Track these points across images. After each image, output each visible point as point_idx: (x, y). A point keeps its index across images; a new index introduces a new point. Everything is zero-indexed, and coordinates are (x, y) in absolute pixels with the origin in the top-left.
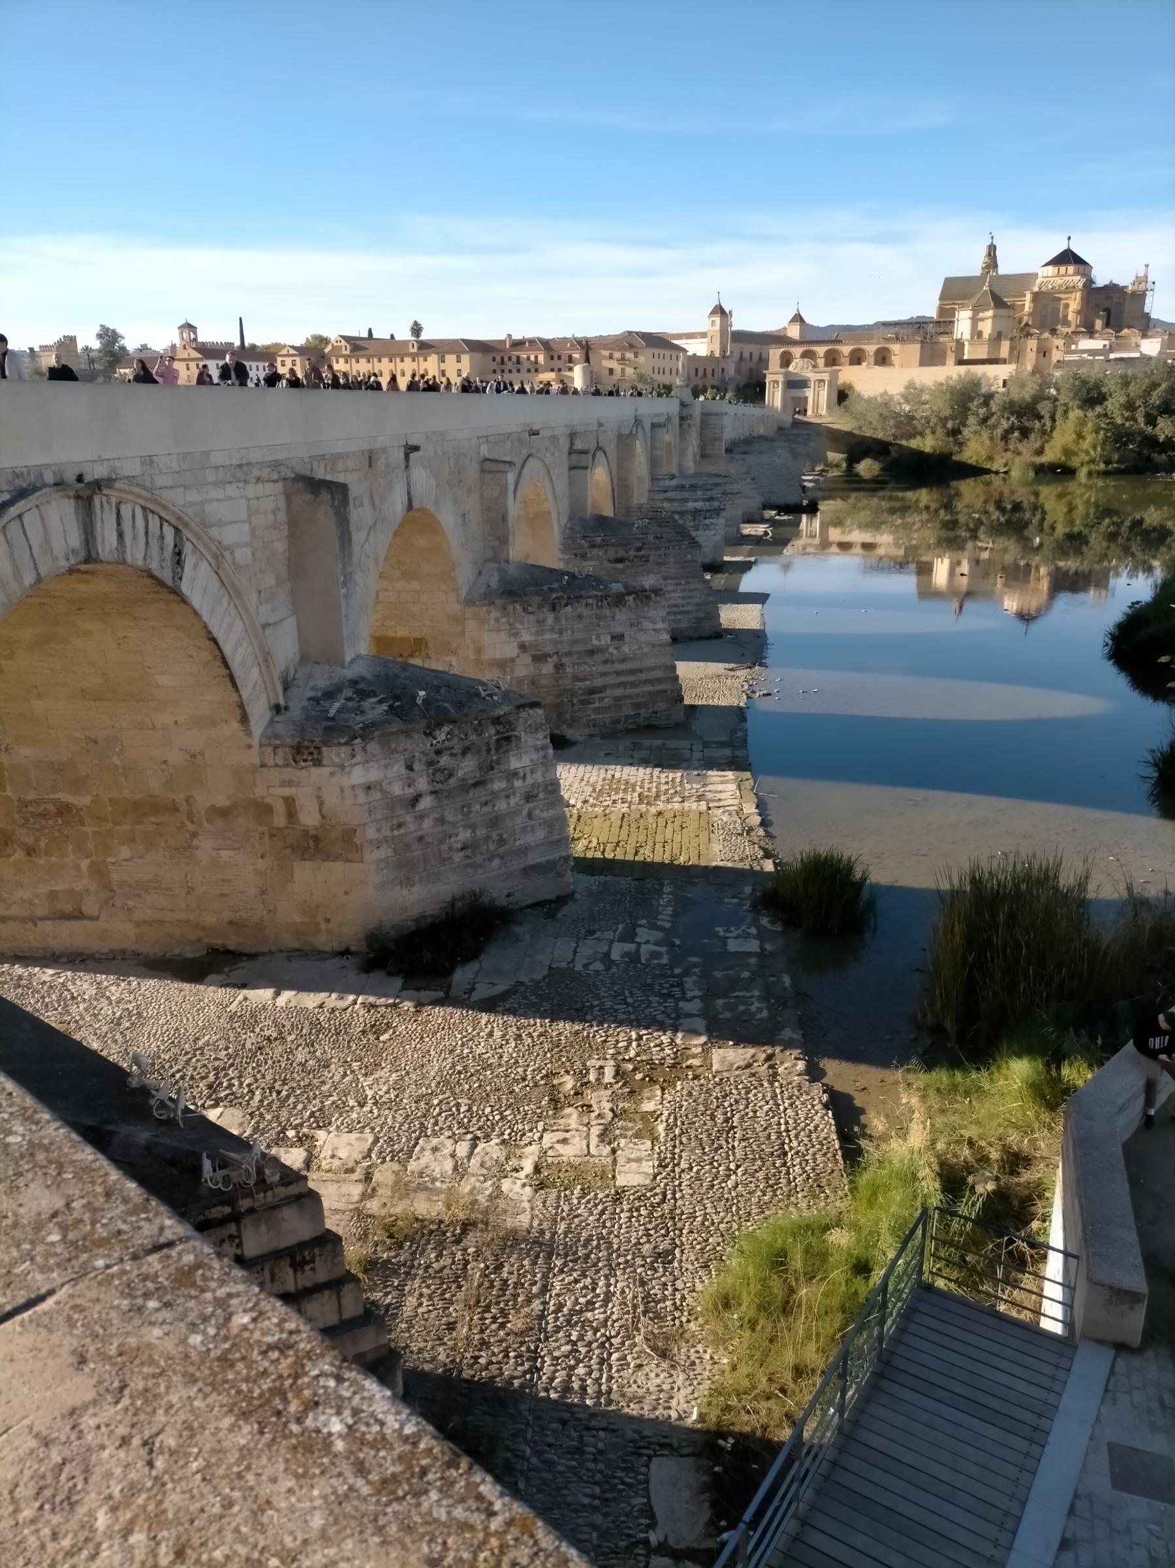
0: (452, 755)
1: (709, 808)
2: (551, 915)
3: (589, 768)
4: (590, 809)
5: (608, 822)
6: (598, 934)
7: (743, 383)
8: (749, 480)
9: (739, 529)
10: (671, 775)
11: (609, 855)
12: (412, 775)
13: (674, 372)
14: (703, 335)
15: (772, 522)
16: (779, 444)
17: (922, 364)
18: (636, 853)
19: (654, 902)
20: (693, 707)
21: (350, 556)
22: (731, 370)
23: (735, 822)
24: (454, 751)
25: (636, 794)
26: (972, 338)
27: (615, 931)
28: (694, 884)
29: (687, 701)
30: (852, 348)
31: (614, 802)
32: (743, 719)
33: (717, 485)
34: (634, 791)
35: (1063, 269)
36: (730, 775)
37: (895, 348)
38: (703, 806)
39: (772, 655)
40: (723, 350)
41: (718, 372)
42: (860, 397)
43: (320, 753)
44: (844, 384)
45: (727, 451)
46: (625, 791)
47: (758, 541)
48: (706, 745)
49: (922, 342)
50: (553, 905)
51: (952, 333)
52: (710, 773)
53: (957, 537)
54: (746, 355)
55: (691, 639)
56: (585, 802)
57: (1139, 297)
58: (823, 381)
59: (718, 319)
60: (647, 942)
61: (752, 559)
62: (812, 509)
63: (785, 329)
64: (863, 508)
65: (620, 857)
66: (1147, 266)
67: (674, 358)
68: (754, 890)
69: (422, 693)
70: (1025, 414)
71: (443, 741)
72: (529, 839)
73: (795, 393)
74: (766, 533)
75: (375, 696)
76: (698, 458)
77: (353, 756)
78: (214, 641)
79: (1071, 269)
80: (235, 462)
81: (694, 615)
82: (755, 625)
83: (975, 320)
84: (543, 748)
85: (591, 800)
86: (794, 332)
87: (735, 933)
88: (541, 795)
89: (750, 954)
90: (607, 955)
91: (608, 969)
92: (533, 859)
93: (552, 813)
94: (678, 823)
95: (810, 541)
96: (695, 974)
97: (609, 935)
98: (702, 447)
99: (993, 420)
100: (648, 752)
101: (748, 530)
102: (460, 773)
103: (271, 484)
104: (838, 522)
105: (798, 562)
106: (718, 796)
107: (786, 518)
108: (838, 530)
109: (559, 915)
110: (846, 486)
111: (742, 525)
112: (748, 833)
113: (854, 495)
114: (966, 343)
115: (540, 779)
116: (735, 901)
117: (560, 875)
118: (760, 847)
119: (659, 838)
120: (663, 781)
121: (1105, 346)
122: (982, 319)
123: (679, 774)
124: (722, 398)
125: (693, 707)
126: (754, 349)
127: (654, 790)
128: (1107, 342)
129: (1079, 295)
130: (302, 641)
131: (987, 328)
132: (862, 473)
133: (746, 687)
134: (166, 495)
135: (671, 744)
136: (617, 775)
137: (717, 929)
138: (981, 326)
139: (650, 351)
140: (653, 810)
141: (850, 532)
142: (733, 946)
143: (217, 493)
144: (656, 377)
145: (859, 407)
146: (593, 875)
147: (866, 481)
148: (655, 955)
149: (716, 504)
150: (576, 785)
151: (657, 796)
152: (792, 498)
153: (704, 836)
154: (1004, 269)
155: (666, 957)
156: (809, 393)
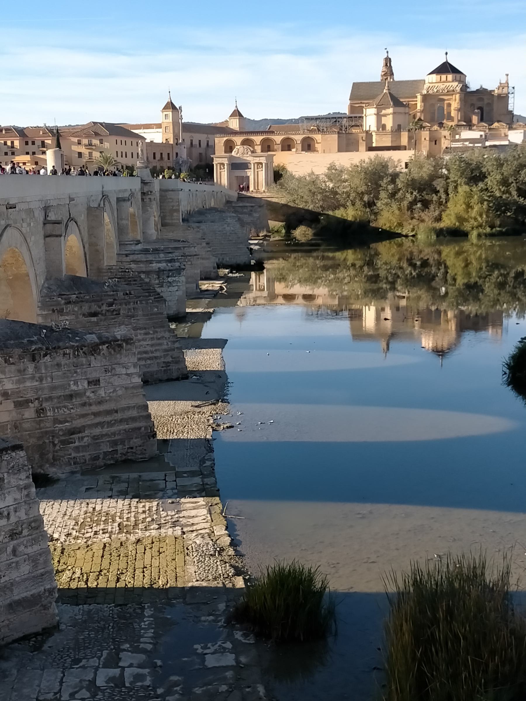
1: (184, 533)
2: (37, 648)
3: (71, 502)
4: (73, 541)
5: (90, 553)
6: (84, 662)
7: (194, 165)
8: (204, 244)
9: (198, 286)
10: (148, 505)
11: (92, 584)
13: (135, 155)
14: (159, 126)
15: (227, 279)
16: (229, 214)
17: (340, 150)
18: (118, 580)
19: (136, 626)
20: (165, 442)
22: (184, 154)
23: (208, 544)
25: (116, 524)
26: (378, 130)
27: (99, 658)
28: (172, 606)
29: (160, 436)
30: (283, 137)
31: (96, 533)
32: (211, 450)
33: (176, 248)
34: (114, 521)
35: (444, 77)
36: (201, 501)
37: (318, 137)
38: (178, 531)
39: (233, 392)
40: (176, 138)
41: (173, 157)
42: (292, 177)
44: (278, 166)
45: (183, 220)
46: (106, 522)
47: (215, 294)
48: (178, 475)
49: (339, 133)
50: (39, 638)
51: (362, 126)
52: (183, 500)
53: (379, 289)
54: (196, 142)
55: (161, 381)
56: (68, 535)
57: (504, 98)
58: (261, 164)
59: (170, 114)
60: (131, 666)
61: (211, 310)
62: (259, 268)
63: (227, 121)
64: (302, 266)
65: (102, 584)
66: (507, 75)
67: (134, 144)
68: (227, 606)
70: (424, 189)
72: (14, 575)
73: (239, 173)
74: (221, 288)
76: (159, 226)
79: (450, 77)
81: (163, 360)
82: (216, 366)
83: (379, 116)
84: (26, 487)
85: (74, 533)
86: (235, 125)
87: (212, 650)
88: (25, 532)
89: (226, 668)
90: (93, 682)
91: (94, 696)
92: (18, 594)
93: (36, 548)
94: (155, 549)
95: (259, 294)
96: (176, 692)
97: (94, 662)
98: (163, 218)
99: (399, 195)
100: (126, 485)
101: (206, 285)
104: (282, 278)
105: (251, 312)
106: (191, 521)
107: (237, 275)
108: (283, 284)
109: (45, 647)
110: (286, 248)
111: (200, 282)
112: (219, 554)
113: (293, 255)
114: (374, 134)
115: (24, 517)
116: (211, 618)
117: (45, 607)
118: (231, 565)
119: (139, 564)
120: (140, 510)
121: (481, 136)
122: (385, 115)
123: (155, 503)
124: (177, 177)
125: (165, 441)
126: (203, 137)
127: (133, 519)
128: (482, 133)
129: (458, 96)
131: (389, 122)
132: (298, 237)
133: (211, 421)
135: (146, 475)
136: (98, 508)
137: (196, 646)
138: (384, 120)
139: (113, 138)
140: (132, 538)
141: (292, 286)
142: (211, 662)
144: (119, 159)
145: (292, 185)
146: (77, 605)
147: (302, 244)
148: (139, 677)
149: (177, 264)
150: (59, 520)
151: (136, 525)
152: (242, 259)
153: (179, 558)
154: (398, 77)
155: (148, 678)
156: (250, 173)
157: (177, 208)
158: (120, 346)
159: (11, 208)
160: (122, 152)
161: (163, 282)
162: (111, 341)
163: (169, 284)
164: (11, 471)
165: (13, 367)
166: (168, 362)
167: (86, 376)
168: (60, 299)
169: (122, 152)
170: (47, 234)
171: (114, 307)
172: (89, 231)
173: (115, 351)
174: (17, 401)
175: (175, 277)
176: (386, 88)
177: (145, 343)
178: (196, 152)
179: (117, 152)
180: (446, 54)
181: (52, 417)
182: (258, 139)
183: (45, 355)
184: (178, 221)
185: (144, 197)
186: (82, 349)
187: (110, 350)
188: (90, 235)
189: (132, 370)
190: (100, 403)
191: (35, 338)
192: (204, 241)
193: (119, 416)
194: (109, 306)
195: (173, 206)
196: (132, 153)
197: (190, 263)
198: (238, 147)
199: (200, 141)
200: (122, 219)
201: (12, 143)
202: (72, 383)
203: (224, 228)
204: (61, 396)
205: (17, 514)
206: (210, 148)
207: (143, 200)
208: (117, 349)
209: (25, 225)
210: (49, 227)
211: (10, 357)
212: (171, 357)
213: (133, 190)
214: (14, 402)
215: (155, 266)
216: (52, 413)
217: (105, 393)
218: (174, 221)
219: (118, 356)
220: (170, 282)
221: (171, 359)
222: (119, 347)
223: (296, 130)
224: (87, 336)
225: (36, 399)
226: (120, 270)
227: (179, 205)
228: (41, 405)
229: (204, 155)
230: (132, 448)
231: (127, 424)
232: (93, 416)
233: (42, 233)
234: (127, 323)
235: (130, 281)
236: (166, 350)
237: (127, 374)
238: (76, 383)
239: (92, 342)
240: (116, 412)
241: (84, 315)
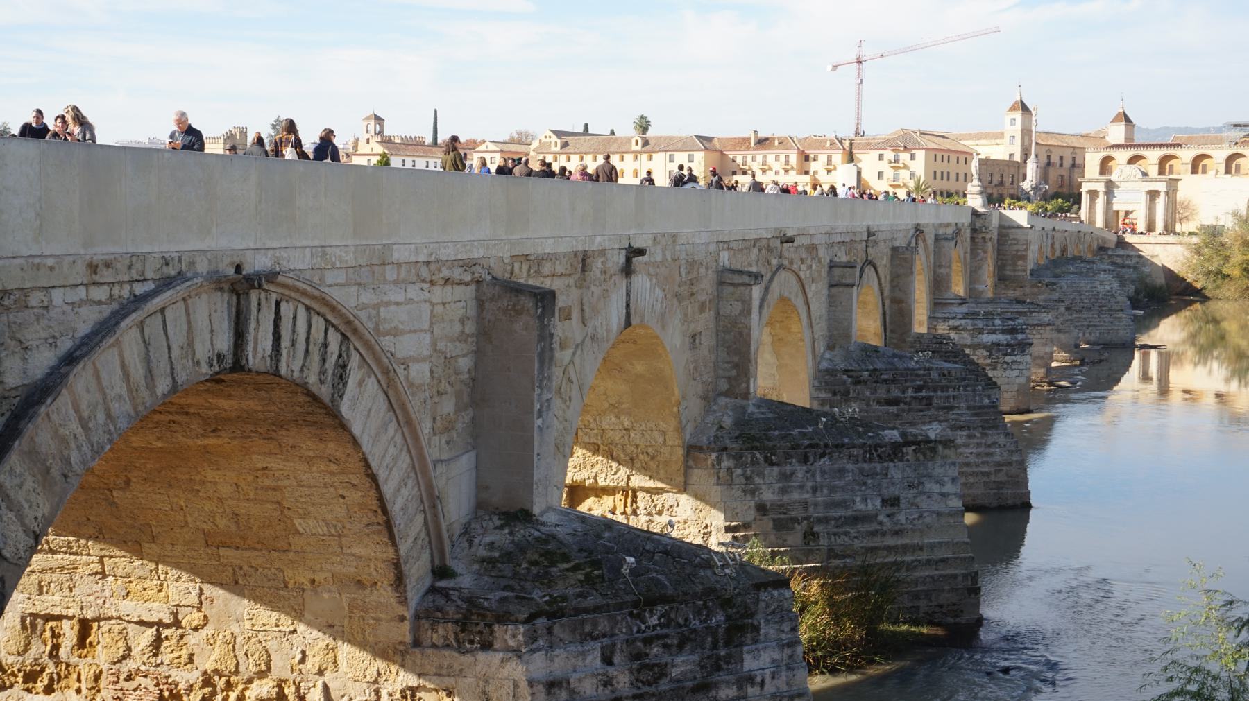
0: (665, 646)
12: (611, 670)
21: (550, 379)
24: (669, 642)
43: (492, 632)
69: (631, 560)
71: (655, 627)
75: (568, 561)
77: (535, 640)
78: (373, 478)
80: (422, 258)
102: (675, 672)
103: (462, 288)
130: (481, 487)
134: (336, 295)
143: (396, 295)
157: (1024, 253)
158: (934, 450)
159: (787, 242)
160: (942, 173)
161: (997, 362)
162: (920, 442)
163: (1005, 366)
164: (769, 618)
165: (776, 469)
166: (1001, 482)
167: (879, 491)
168: (845, 377)
169: (942, 173)
170: (833, 282)
171: (924, 393)
172: (892, 281)
173: (925, 455)
174: (779, 519)
175: (1015, 355)
177: (967, 451)
178: (1053, 174)
179: (935, 172)
181: (825, 548)
182: (1154, 156)
183: (822, 456)
184: (1024, 274)
185: (975, 235)
186: (876, 451)
187: (918, 455)
188: (893, 288)
189: (949, 488)
190: (897, 533)
191: (810, 429)
192: (1063, 304)
193: (924, 556)
194: (916, 392)
195: (1017, 251)
196: (957, 174)
197: (1039, 336)
198: (1122, 167)
199: (1061, 158)
200: (940, 266)
201: (787, 157)
202: (858, 499)
203: (1095, 287)
204: (840, 517)
205: (775, 681)
206: (1077, 166)
207: (973, 239)
208: (928, 453)
209: (804, 267)
210: (837, 271)
211: (772, 454)
212: (1007, 475)
213: (960, 225)
214: (774, 520)
215: (987, 338)
216: (826, 541)
217: (907, 518)
218: (1017, 274)
219: (930, 464)
220: (1008, 364)
221: (1006, 478)
222: (931, 452)
223: (1217, 141)
224: (886, 431)
225: (804, 519)
226: (934, 341)
227: (1026, 250)
228: (812, 529)
229: (1066, 178)
230: (941, 606)
231: (936, 569)
232: (885, 552)
233: (826, 281)
234: (942, 418)
235: (949, 357)
236: (998, 464)
237: (943, 495)
238: (864, 500)
239: (893, 441)
240: (921, 549)
241: (879, 403)
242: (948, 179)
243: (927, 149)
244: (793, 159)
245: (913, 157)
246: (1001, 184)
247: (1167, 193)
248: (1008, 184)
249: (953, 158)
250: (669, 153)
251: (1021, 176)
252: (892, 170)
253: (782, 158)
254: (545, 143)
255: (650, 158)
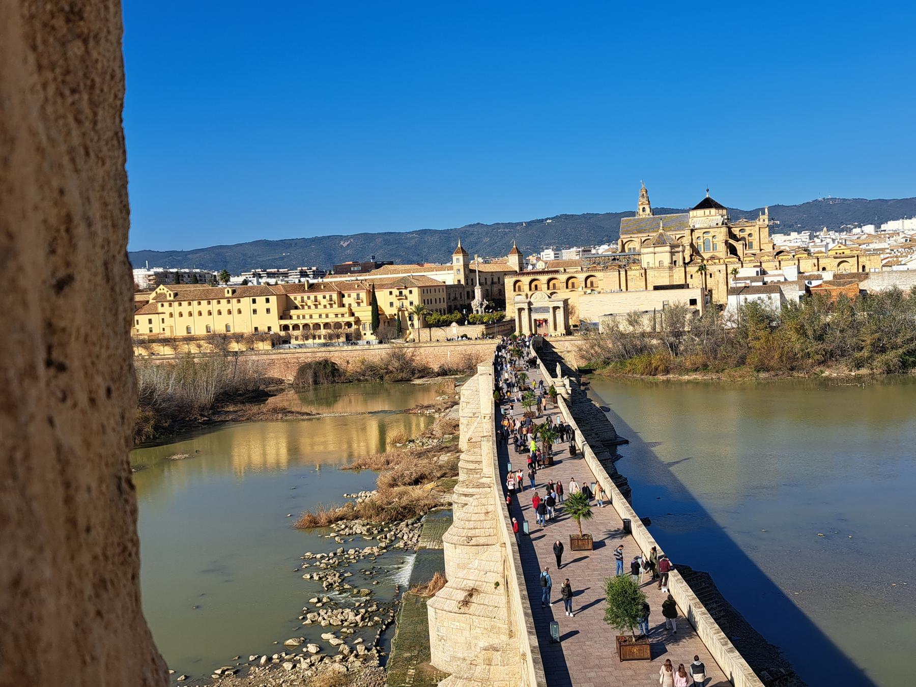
176: (661, 228)
179: (424, 300)
180: (708, 190)
199: (486, 279)
201: (331, 296)
229: (490, 290)
242: (431, 303)
243: (419, 287)
244: (335, 296)
245: (411, 292)
246: (455, 299)
247: (564, 307)
248: (459, 298)
249: (433, 291)
250: (251, 298)
251: (466, 293)
252: (398, 301)
253: (328, 297)
254: (160, 294)
255: (239, 301)
